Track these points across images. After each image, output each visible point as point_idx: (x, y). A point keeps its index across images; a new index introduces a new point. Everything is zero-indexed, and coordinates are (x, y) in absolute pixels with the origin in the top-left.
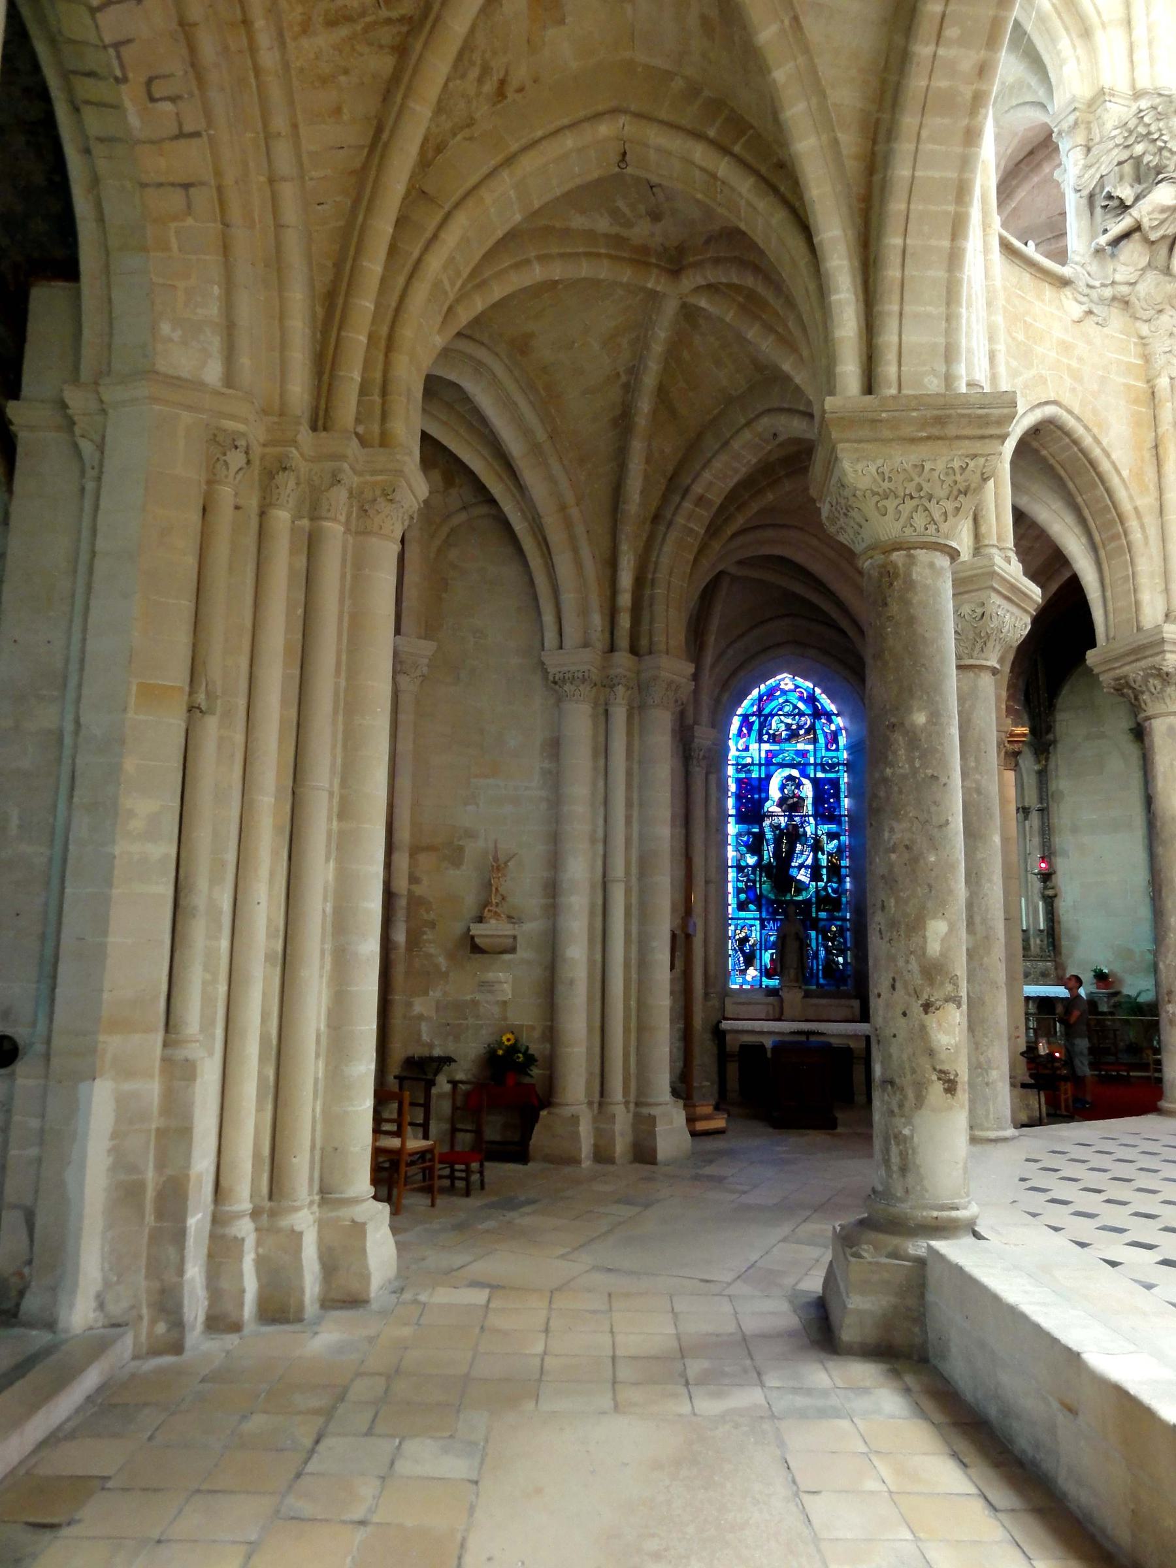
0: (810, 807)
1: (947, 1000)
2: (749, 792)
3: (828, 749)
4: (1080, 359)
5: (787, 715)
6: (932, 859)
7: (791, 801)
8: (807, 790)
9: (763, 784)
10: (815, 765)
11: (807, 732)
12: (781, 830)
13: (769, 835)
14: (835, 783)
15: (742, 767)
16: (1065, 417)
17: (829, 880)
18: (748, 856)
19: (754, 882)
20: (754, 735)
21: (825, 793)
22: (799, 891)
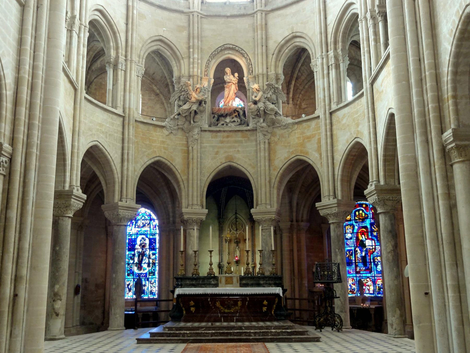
0: (148, 246)
1: (58, 299)
2: (132, 242)
3: (153, 230)
4: (168, 145)
5: (143, 220)
6: (57, 274)
7: (143, 245)
8: (147, 241)
9: (135, 240)
10: (150, 234)
11: (148, 225)
12: (140, 253)
13: (137, 255)
14: (155, 239)
15: (131, 235)
16: (161, 159)
17: (152, 267)
18: (131, 260)
19: (132, 268)
20: (134, 226)
21: (152, 242)
22: (144, 270)
